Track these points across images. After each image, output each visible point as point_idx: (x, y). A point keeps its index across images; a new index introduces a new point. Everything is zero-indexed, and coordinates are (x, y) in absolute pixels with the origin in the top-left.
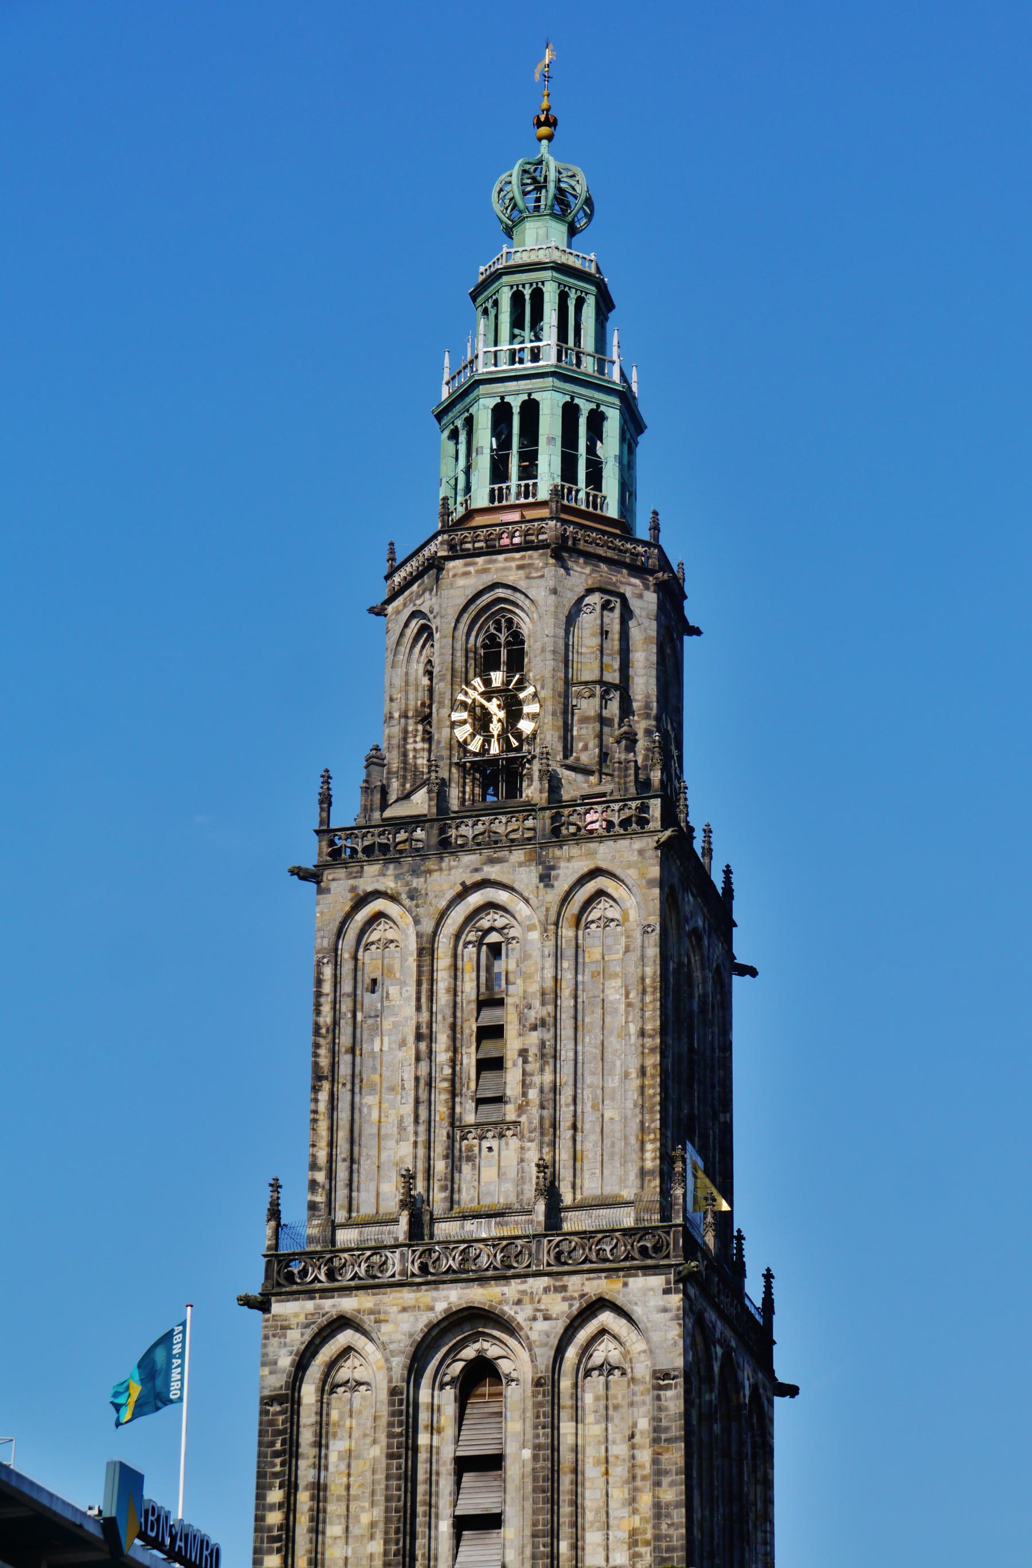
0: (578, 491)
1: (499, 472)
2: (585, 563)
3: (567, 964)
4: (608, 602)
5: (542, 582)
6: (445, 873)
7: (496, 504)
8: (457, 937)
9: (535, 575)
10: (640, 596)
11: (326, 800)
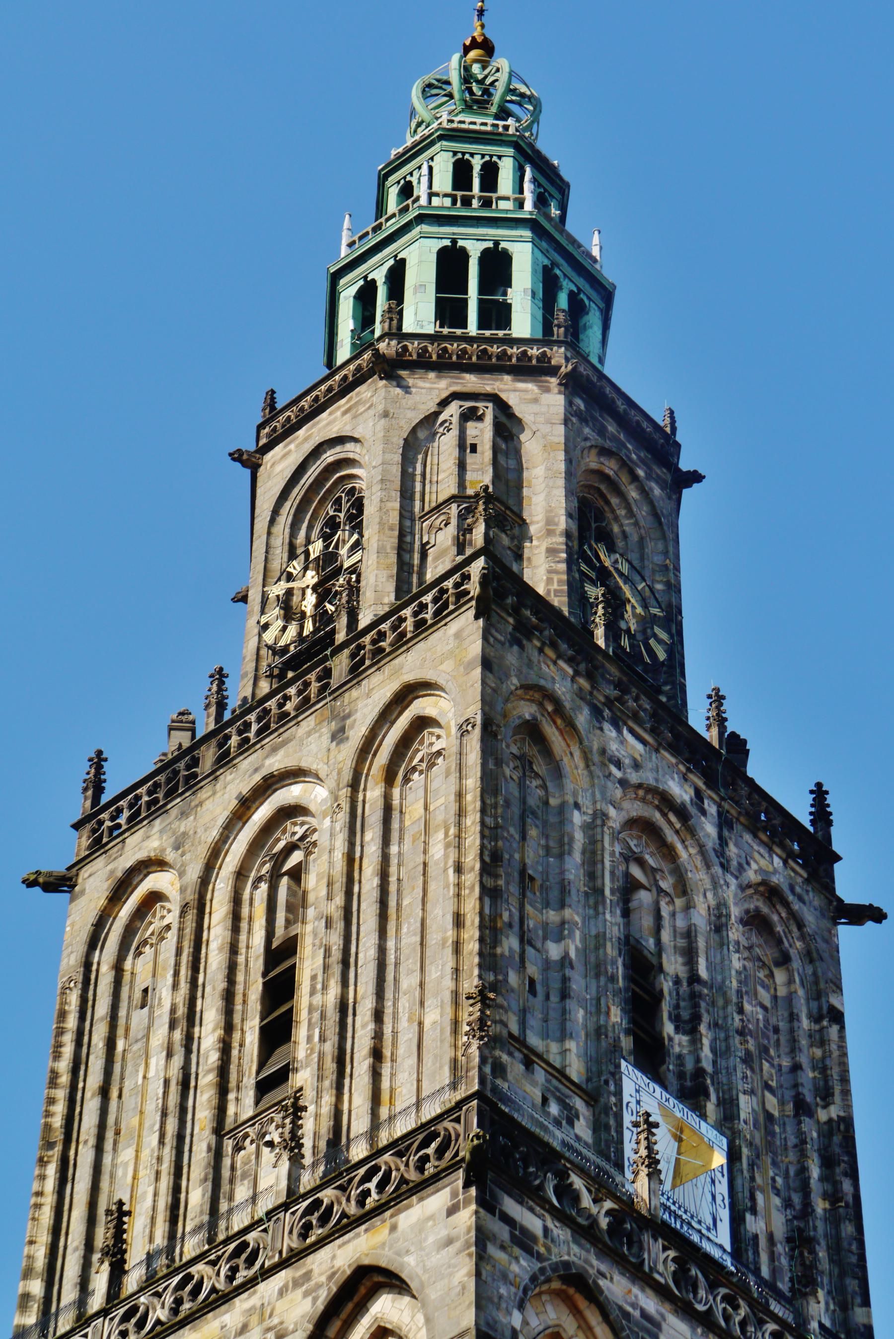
3: (372, 837)
4: (474, 410)
5: (371, 412)
6: (218, 795)
8: (240, 875)
10: (536, 401)
11: (97, 786)
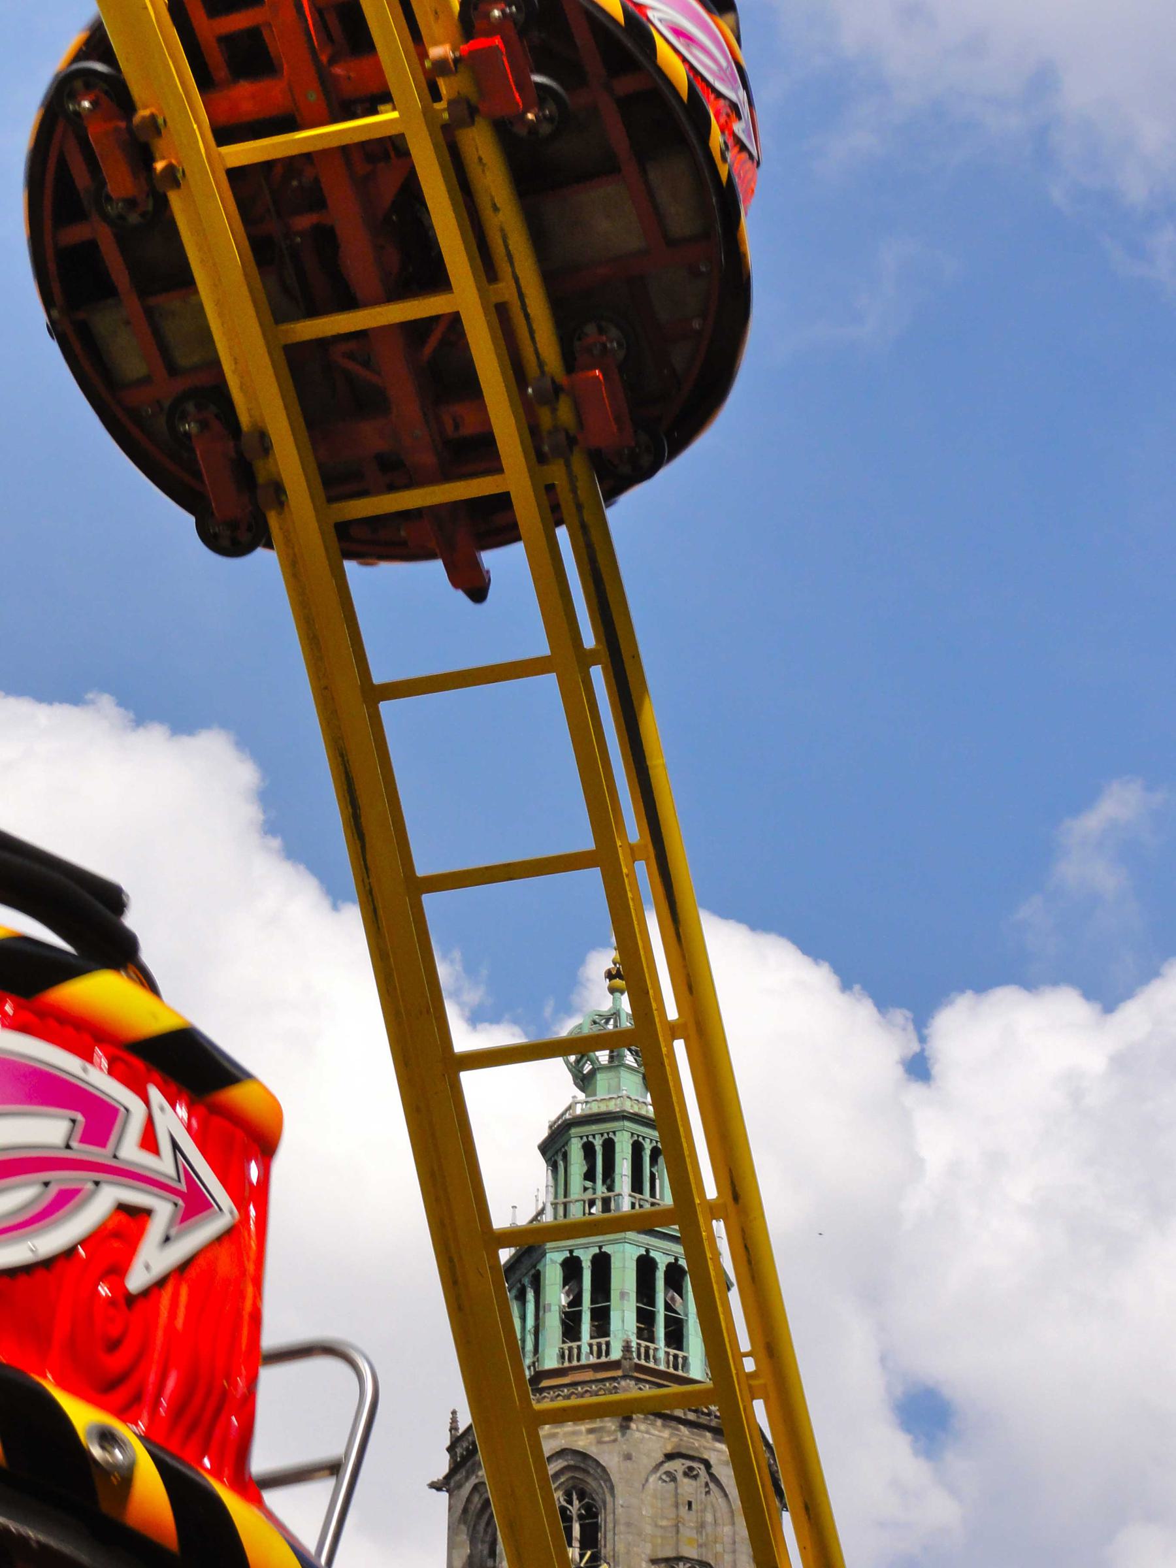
0: (656, 1350)
1: (571, 1329)
2: (664, 1426)
4: (691, 1469)
7: (567, 1364)
9: (607, 1439)
